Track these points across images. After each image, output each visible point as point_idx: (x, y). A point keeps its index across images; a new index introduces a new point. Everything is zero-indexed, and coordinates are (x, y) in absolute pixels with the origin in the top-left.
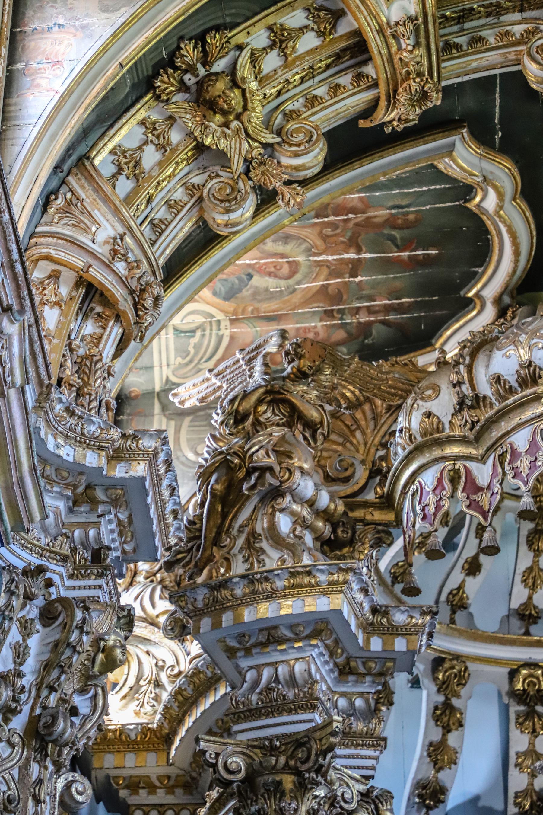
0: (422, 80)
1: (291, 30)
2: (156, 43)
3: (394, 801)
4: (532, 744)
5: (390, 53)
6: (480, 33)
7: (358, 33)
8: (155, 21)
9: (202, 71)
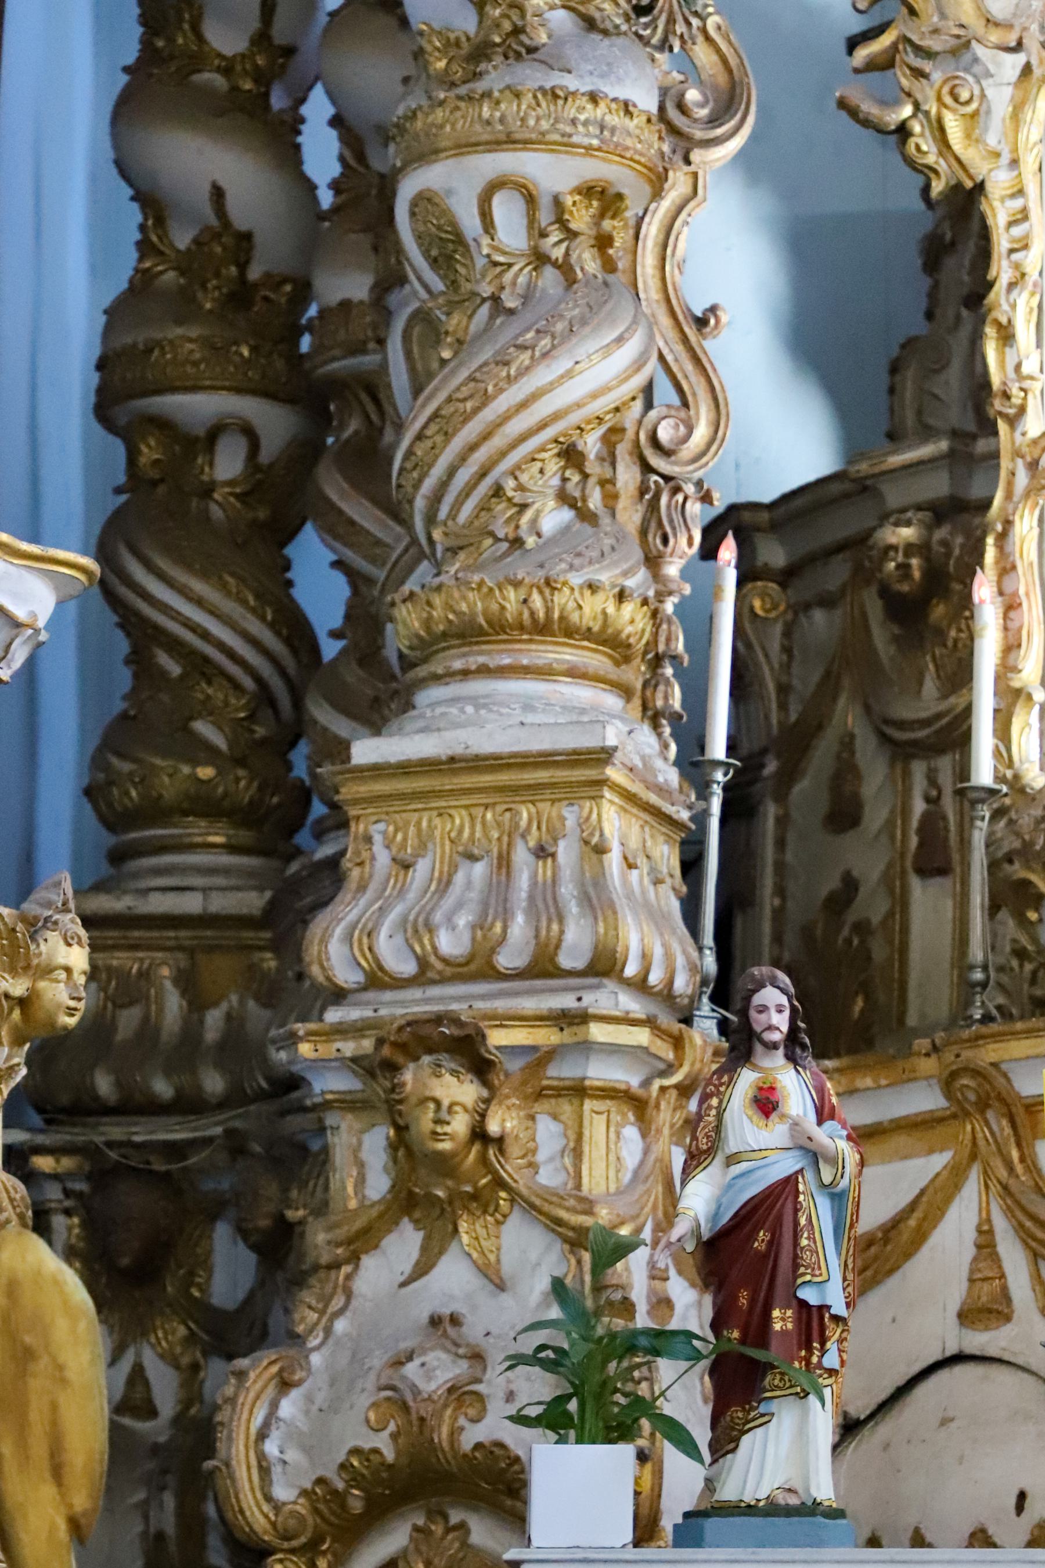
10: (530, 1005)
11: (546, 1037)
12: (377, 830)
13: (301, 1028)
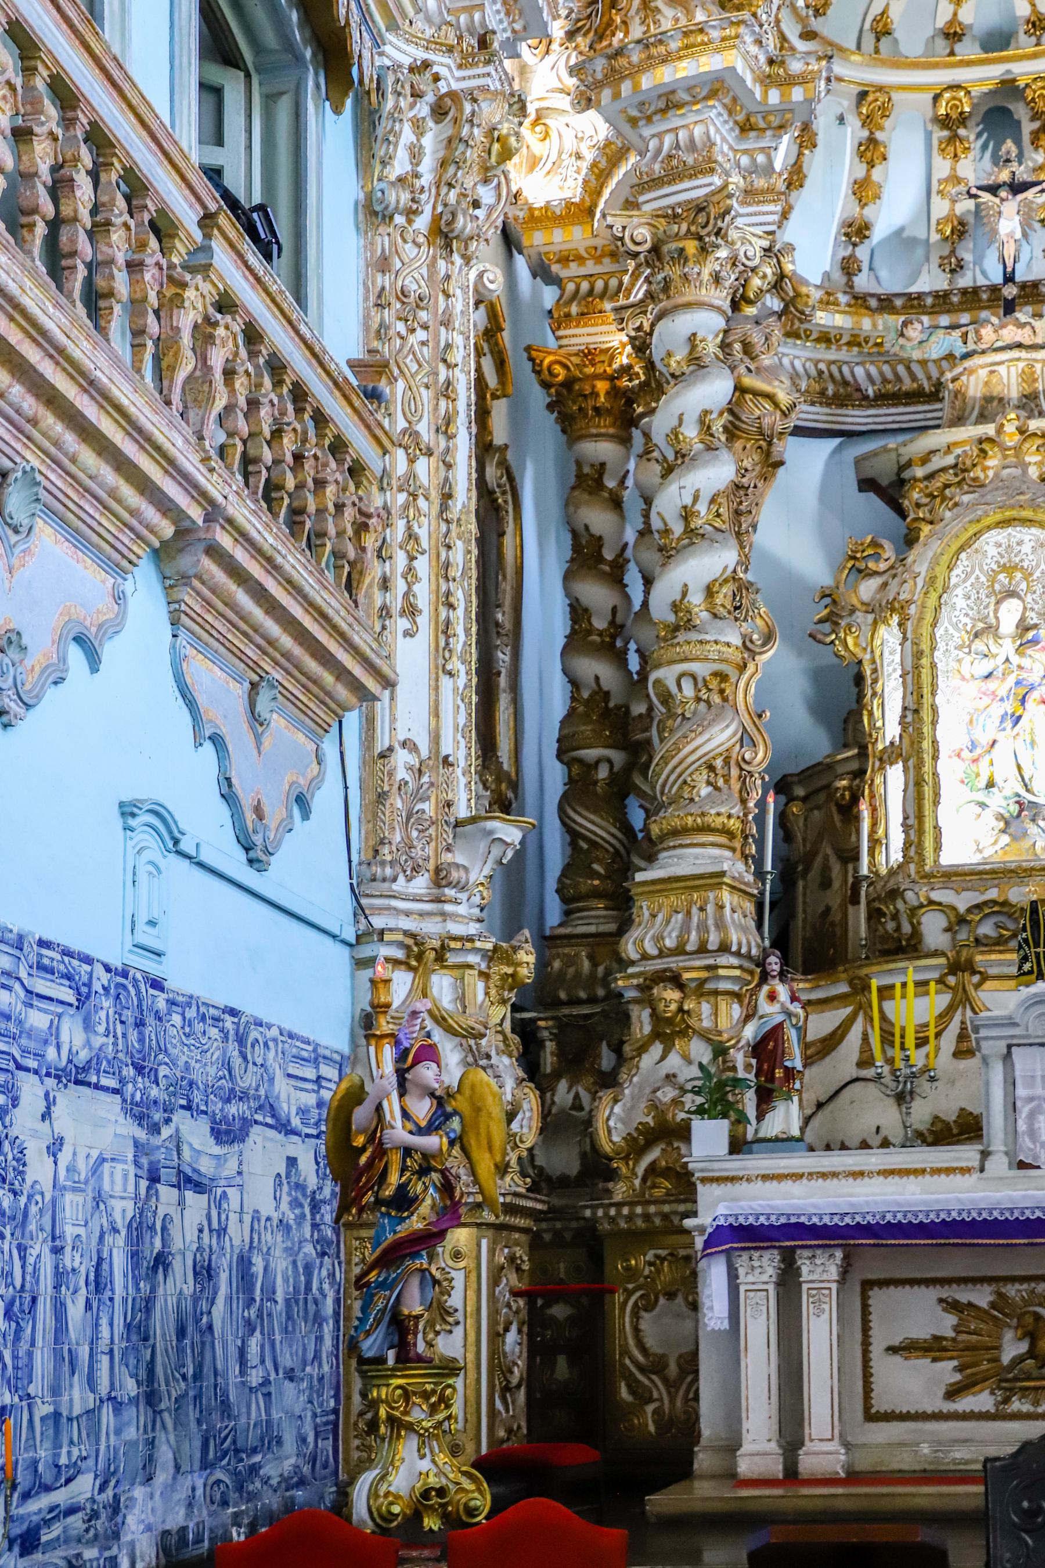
3: (796, 253)
4: (953, 169)
10: (698, 963)
11: (704, 974)
12: (644, 904)
13: (618, 975)
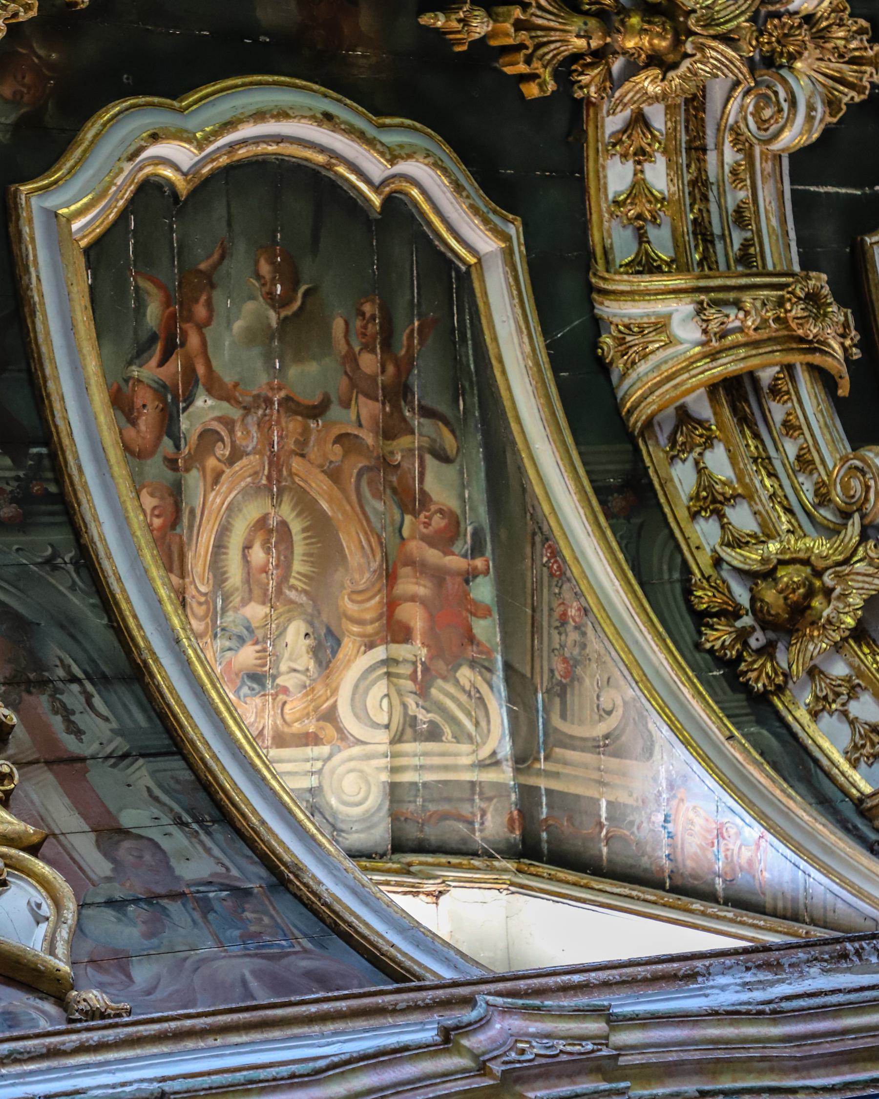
0: (789, 300)
1: (699, 485)
2: (702, 683)
5: (745, 345)
6: (730, 210)
7: (713, 389)
8: (671, 683)
9: (747, 621)
